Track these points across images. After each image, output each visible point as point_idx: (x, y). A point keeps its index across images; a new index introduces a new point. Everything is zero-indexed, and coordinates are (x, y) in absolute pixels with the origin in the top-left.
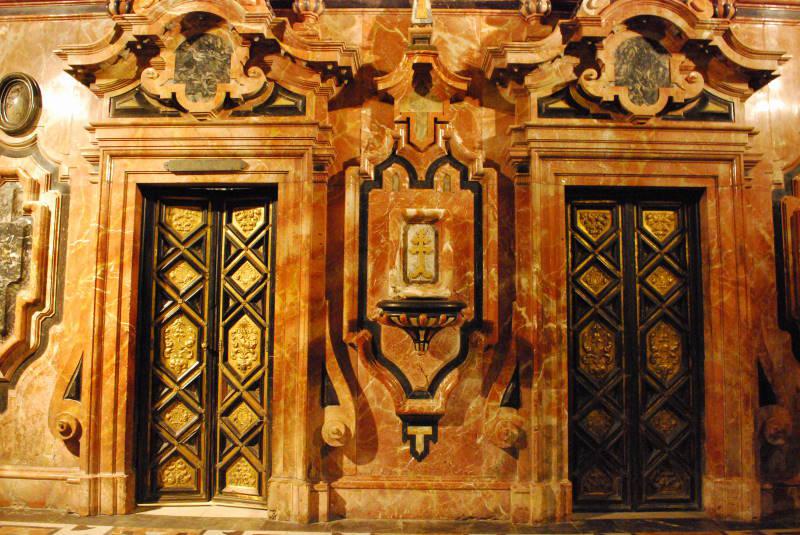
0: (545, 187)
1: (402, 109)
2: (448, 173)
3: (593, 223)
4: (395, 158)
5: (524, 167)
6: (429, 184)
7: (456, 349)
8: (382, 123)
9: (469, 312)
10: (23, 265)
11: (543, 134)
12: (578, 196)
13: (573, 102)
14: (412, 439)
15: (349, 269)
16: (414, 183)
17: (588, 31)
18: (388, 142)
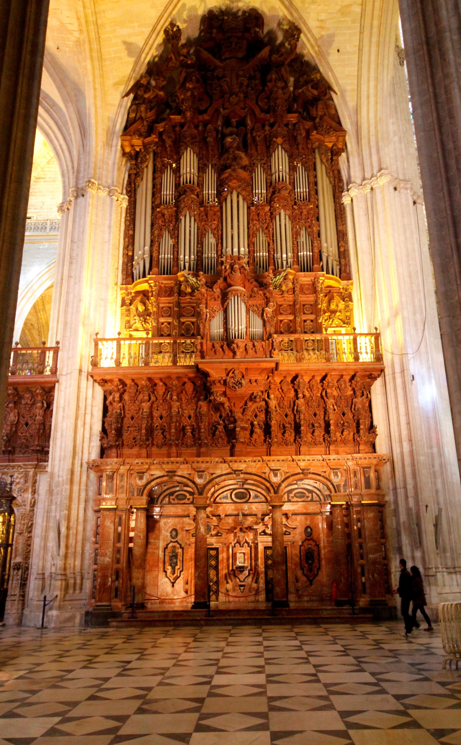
0: (261, 548)
1: (238, 534)
2: (246, 544)
3: (269, 552)
4: (237, 542)
5: (257, 544)
6: (243, 547)
7: (247, 574)
8: (235, 536)
9: (249, 568)
10: (177, 562)
11: (261, 538)
12: (266, 548)
13: (264, 533)
14: (240, 589)
15: (231, 561)
16: (240, 546)
18: (236, 540)
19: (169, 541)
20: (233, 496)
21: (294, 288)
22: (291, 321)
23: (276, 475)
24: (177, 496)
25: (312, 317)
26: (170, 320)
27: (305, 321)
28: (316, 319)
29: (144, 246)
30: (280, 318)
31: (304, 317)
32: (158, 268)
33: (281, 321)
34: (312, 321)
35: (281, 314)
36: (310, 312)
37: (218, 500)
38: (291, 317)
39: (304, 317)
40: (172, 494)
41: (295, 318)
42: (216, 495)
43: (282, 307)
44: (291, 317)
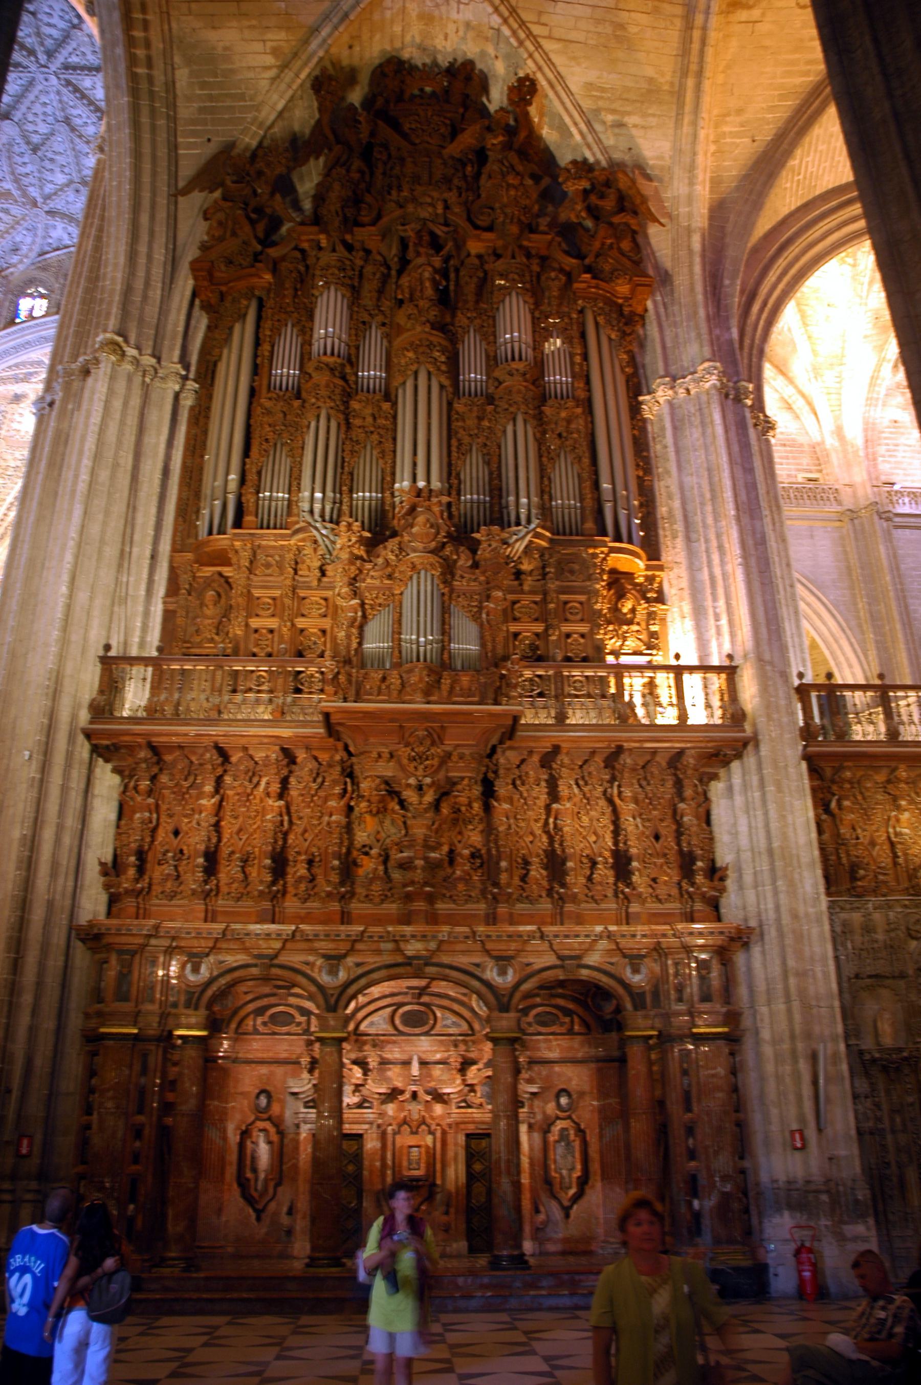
17: (469, 1082)
19: (252, 1118)
20: (397, 1021)
21: (544, 567)
22: (537, 635)
23: (503, 972)
24: (273, 1016)
25: (584, 628)
26: (273, 623)
27: (568, 636)
28: (592, 632)
29: (227, 473)
30: (513, 628)
31: (566, 628)
32: (257, 516)
33: (516, 635)
34: (583, 636)
35: (515, 619)
36: (579, 617)
37: (363, 1027)
38: (539, 628)
39: (566, 628)
40: (260, 1011)
41: (546, 630)
42: (360, 1015)
43: (517, 606)
44: (539, 628)
